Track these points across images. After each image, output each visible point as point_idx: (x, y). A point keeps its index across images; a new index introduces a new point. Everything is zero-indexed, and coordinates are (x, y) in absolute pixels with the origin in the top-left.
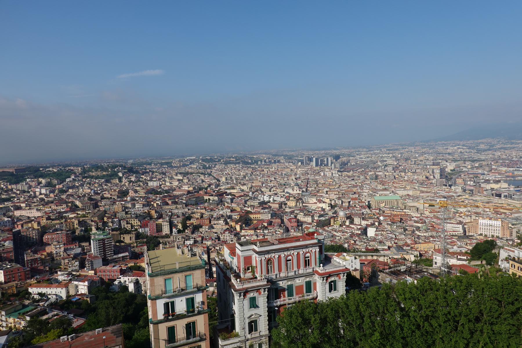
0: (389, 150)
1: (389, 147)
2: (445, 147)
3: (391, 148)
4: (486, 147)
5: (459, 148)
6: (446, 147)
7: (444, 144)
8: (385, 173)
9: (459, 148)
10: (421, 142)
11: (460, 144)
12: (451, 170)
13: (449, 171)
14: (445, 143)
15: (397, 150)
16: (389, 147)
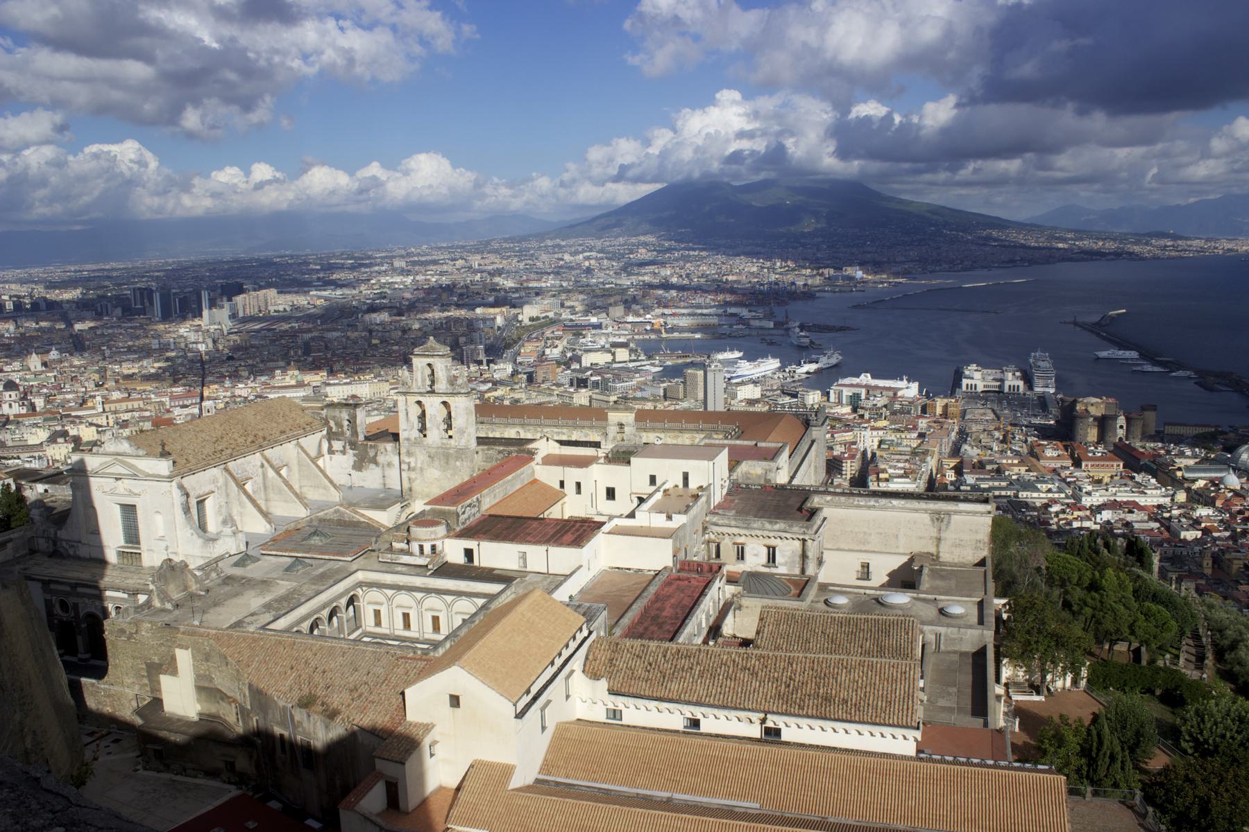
0: (414, 263)
1: (419, 254)
2: (556, 256)
3: (423, 259)
4: (649, 254)
5: (588, 258)
6: (560, 256)
7: (559, 246)
8: (349, 334)
9: (588, 258)
10: (506, 240)
11: (594, 247)
12: (532, 319)
13: (526, 322)
14: (563, 243)
15: (435, 262)
16: (419, 254)
